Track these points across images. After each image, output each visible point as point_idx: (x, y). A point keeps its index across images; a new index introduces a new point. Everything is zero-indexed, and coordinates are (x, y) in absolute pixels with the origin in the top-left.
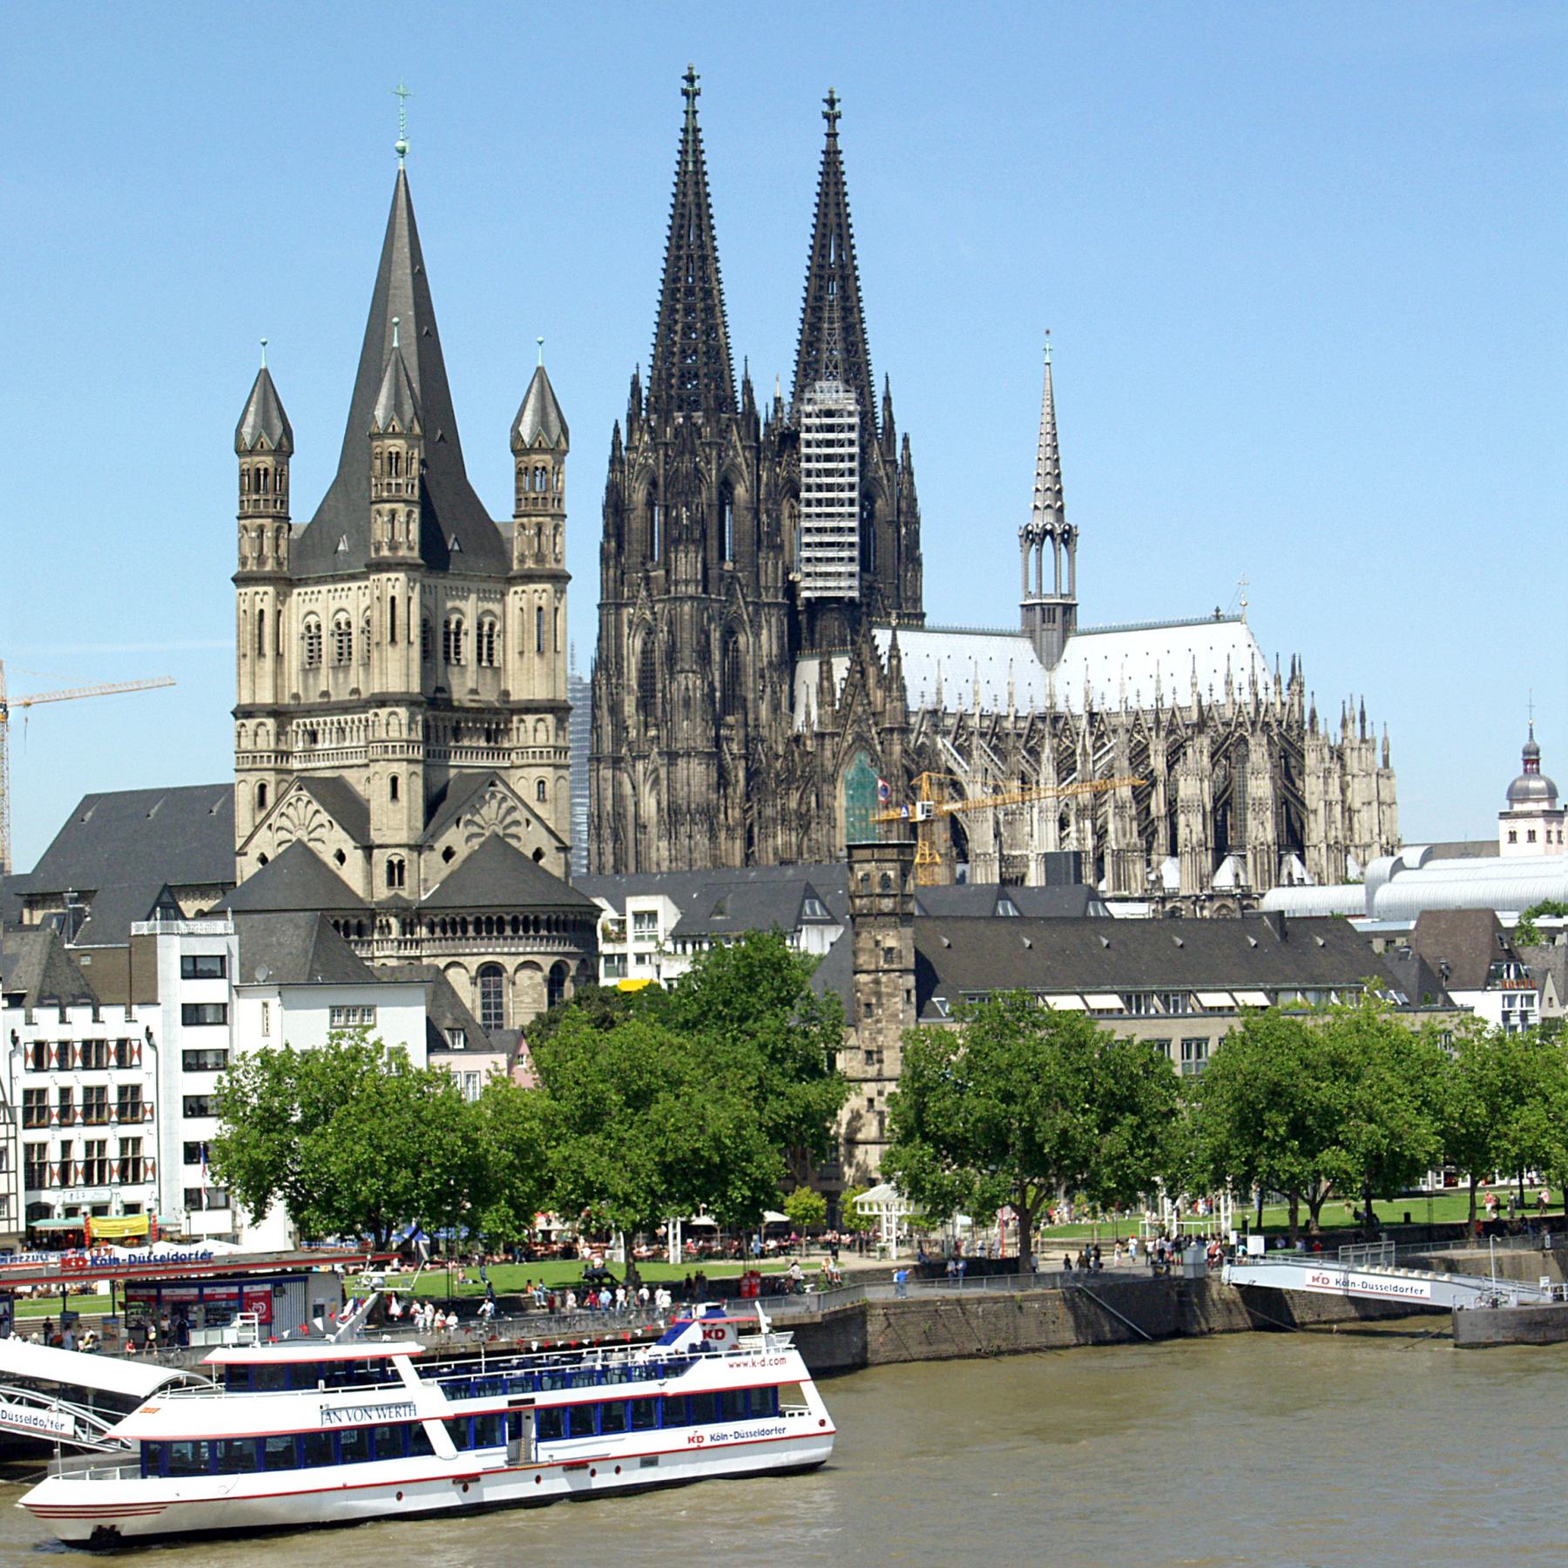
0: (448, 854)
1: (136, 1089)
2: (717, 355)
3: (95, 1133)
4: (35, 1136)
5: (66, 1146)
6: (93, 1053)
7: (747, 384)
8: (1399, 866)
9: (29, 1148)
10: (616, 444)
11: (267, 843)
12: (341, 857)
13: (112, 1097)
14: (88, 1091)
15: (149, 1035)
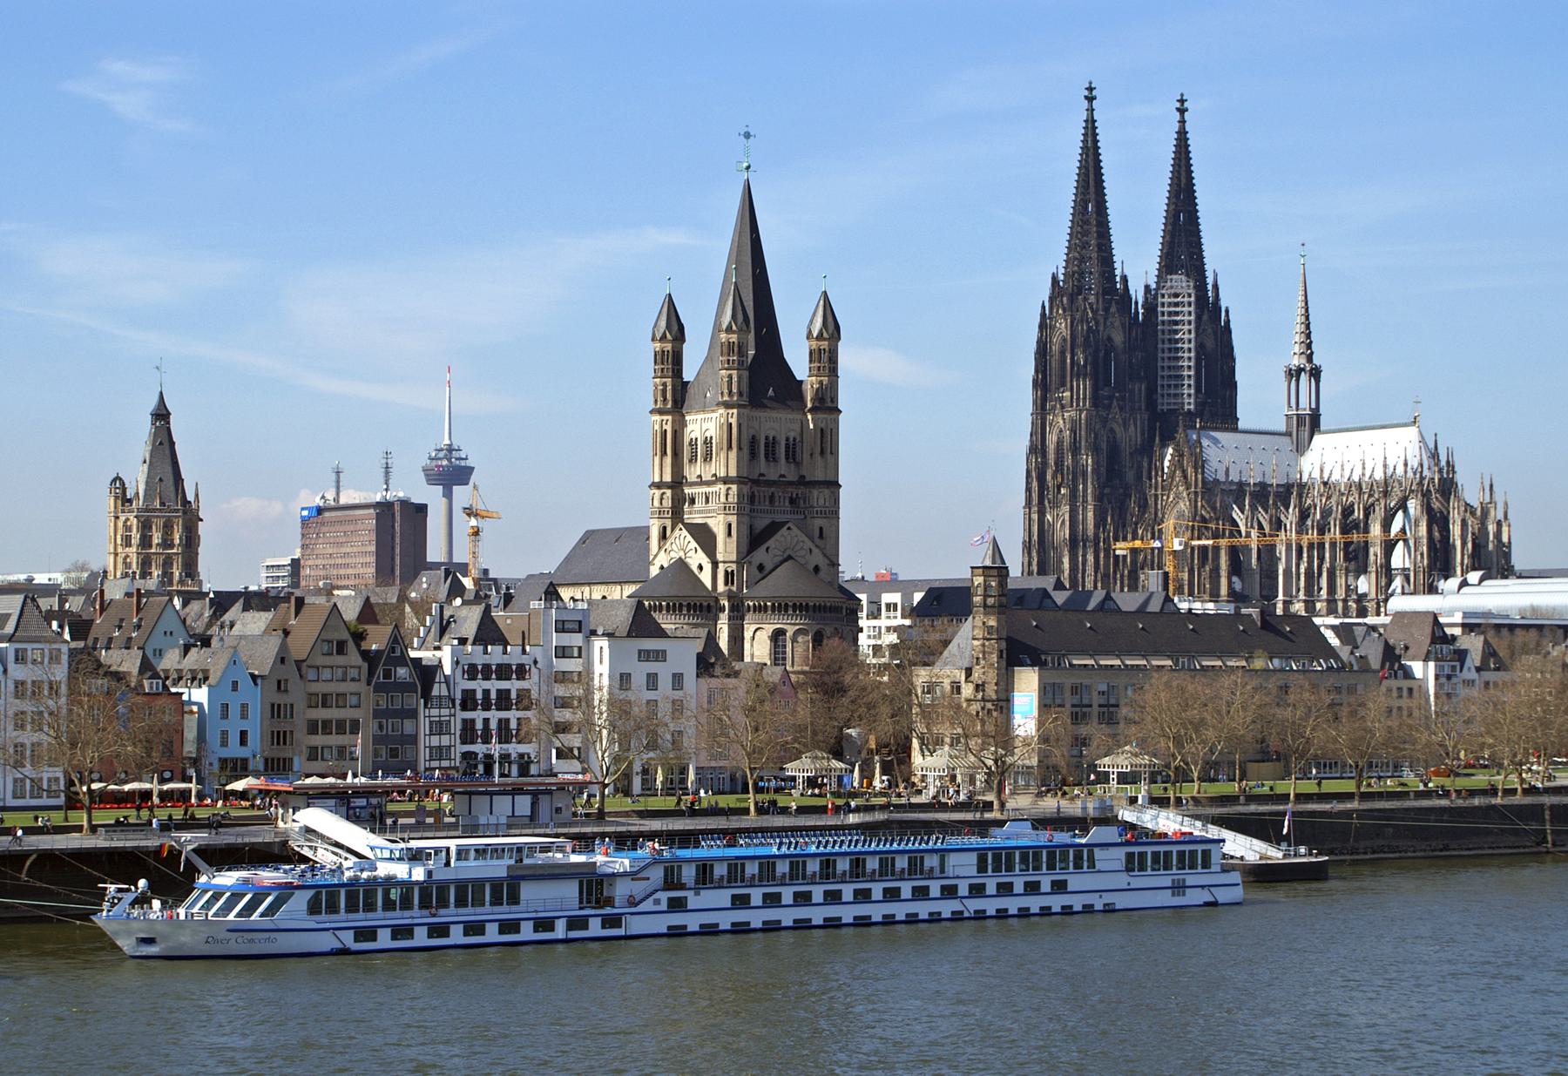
0: (761, 568)
1: (528, 691)
2: (1107, 260)
3: (504, 714)
4: (469, 715)
5: (486, 721)
6: (503, 672)
7: (1125, 279)
8: (1464, 584)
9: (465, 721)
10: (1043, 315)
11: (663, 560)
12: (700, 567)
13: (513, 695)
14: (499, 691)
15: (535, 662)
